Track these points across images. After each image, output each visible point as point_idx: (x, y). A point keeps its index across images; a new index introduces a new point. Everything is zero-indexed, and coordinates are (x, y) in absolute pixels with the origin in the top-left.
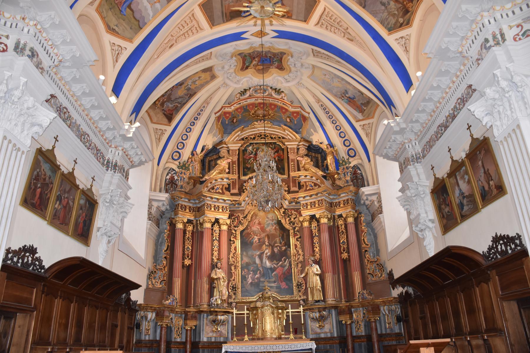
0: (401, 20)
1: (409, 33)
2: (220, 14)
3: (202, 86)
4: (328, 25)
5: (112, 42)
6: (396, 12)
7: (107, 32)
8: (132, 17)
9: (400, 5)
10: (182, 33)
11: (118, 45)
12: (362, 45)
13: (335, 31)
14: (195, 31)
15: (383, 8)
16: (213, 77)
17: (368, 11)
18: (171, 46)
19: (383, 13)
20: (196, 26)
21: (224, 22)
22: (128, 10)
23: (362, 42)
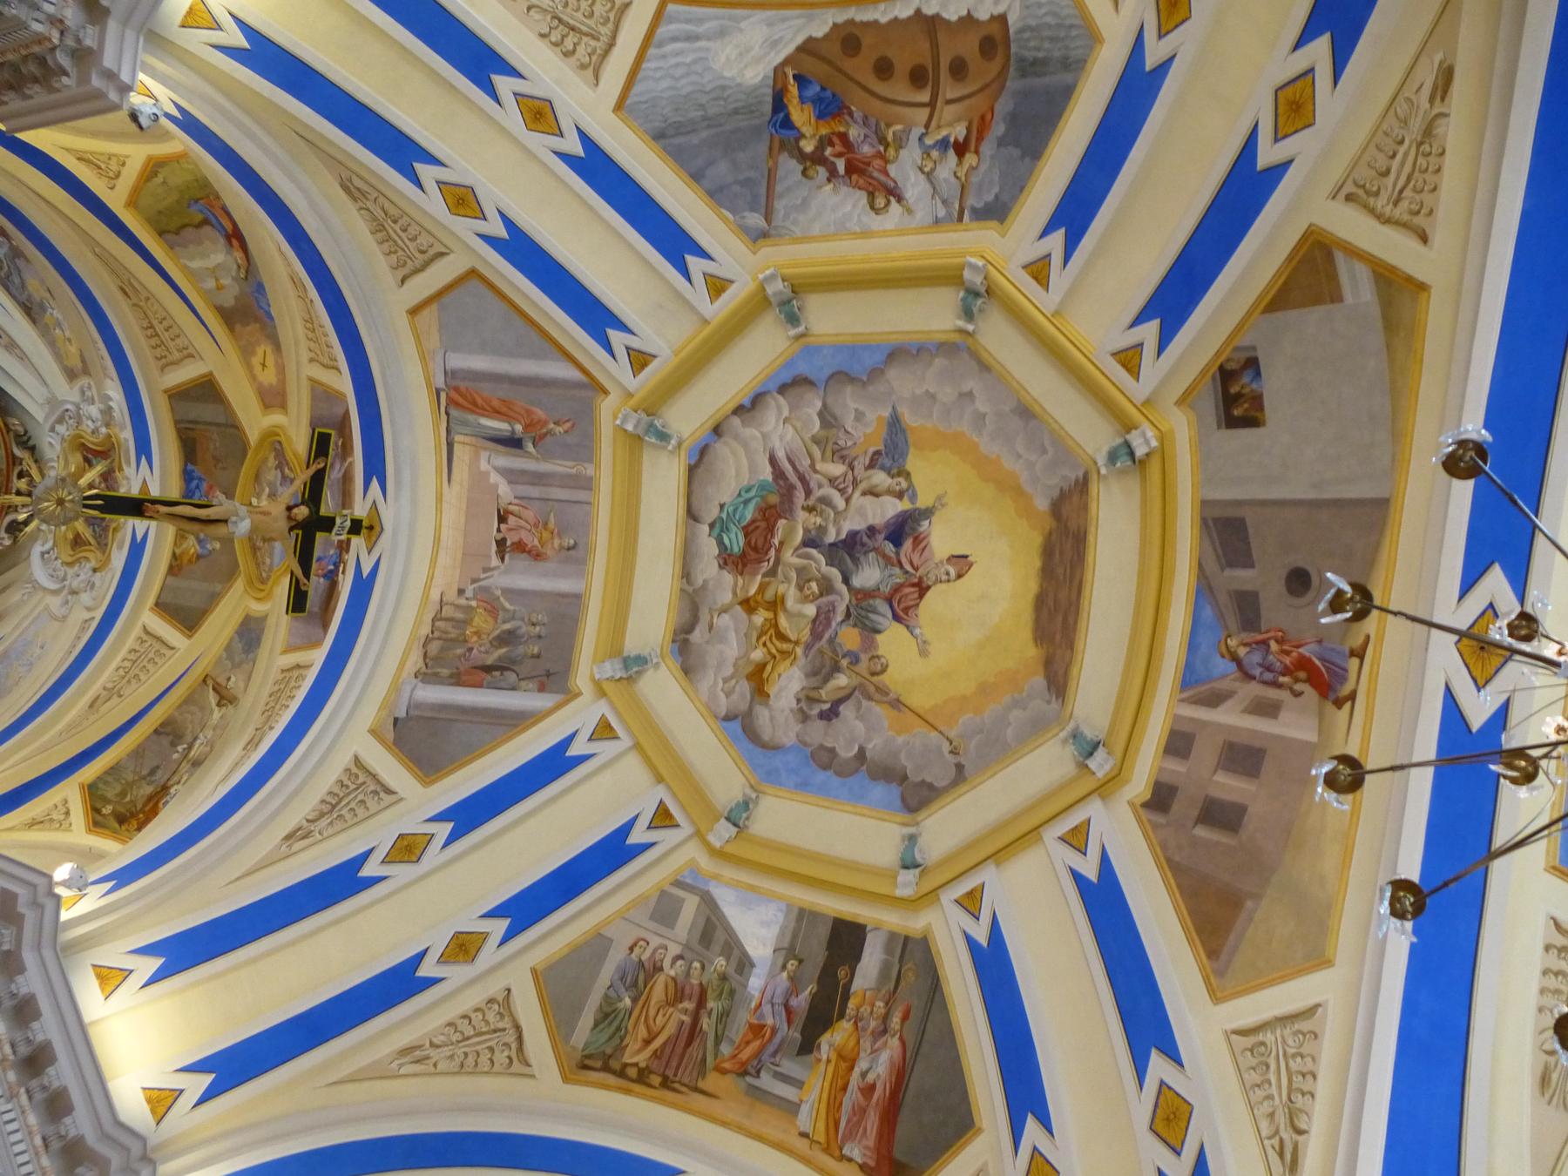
0: (107, 810)
1: (73, 827)
2: (192, 416)
3: (52, 344)
4: (139, 654)
5: (128, 162)
6: (128, 799)
7: (150, 158)
8: (186, 221)
9: (139, 807)
10: (155, 323)
11: (119, 172)
12: (73, 728)
13: (121, 670)
14: (158, 352)
15: (145, 772)
16: (71, 375)
17: (148, 738)
18: (125, 293)
19: (134, 772)
20: (170, 358)
21: (176, 422)
22: (200, 217)
23: (81, 728)
